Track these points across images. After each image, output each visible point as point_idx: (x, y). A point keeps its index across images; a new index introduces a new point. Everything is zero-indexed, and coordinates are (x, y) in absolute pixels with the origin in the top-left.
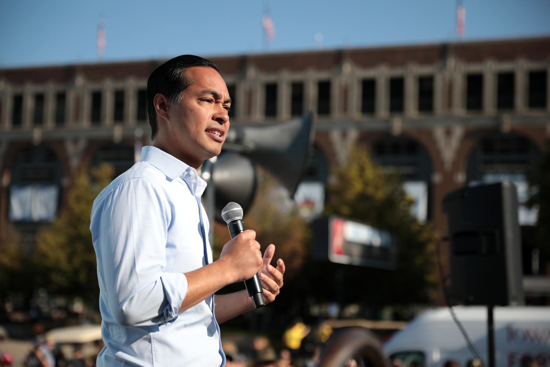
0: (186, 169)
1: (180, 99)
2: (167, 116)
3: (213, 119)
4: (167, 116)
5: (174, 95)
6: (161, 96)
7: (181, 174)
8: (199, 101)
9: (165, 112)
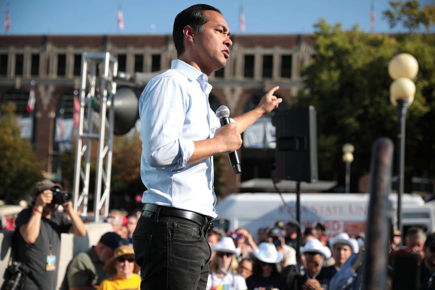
0: (200, 75)
3: (224, 43)
7: (197, 78)
8: (215, 31)
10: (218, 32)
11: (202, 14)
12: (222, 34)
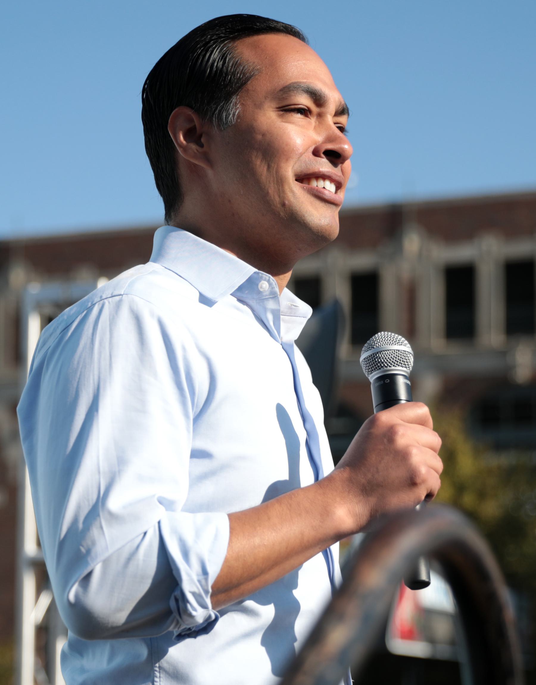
0: (250, 275)
1: (234, 115)
2: (207, 158)
4: (207, 158)
5: (216, 108)
6: (189, 112)
9: (200, 150)
10: (298, 117)
11: (223, 57)
12: (313, 120)
